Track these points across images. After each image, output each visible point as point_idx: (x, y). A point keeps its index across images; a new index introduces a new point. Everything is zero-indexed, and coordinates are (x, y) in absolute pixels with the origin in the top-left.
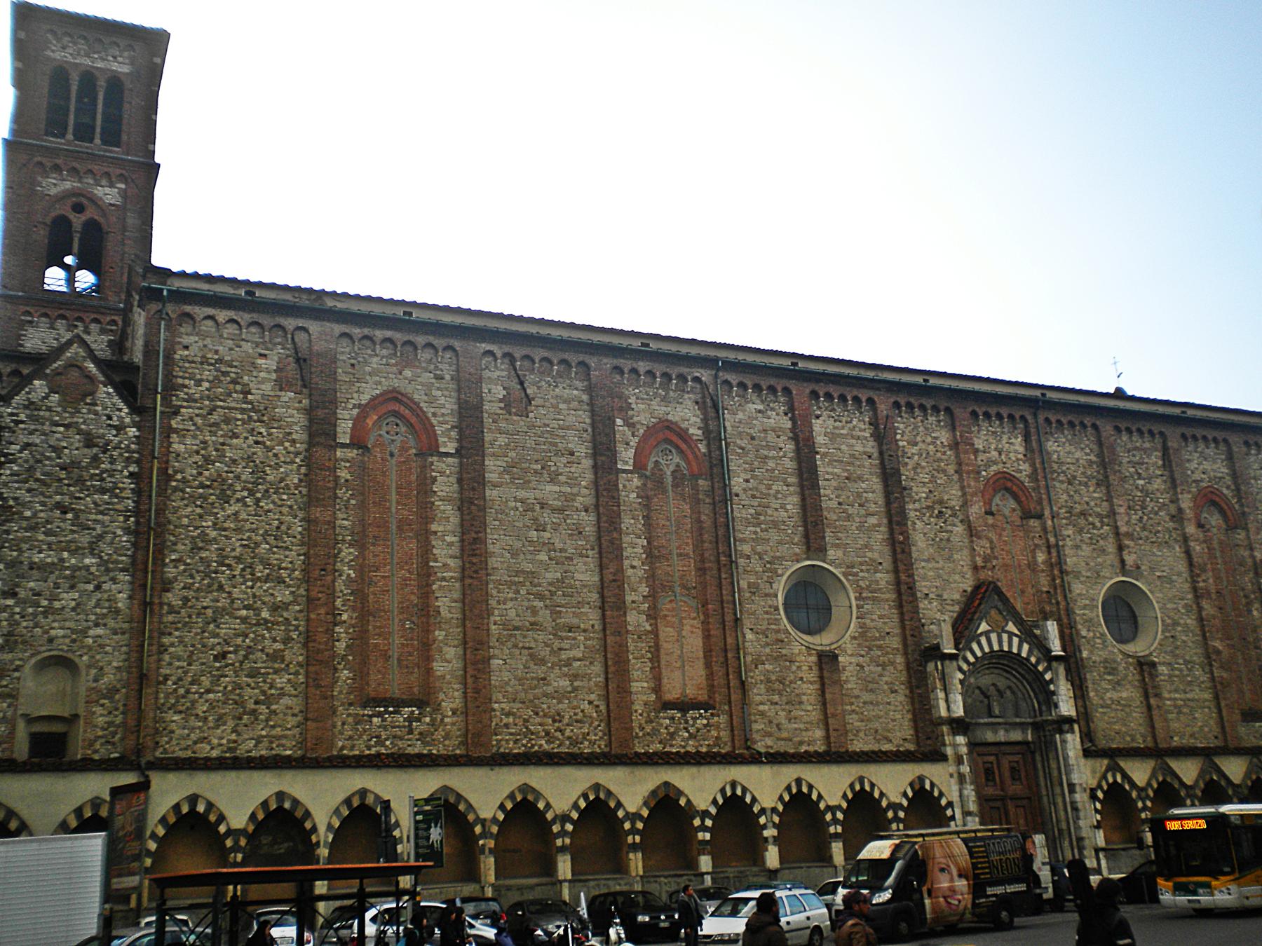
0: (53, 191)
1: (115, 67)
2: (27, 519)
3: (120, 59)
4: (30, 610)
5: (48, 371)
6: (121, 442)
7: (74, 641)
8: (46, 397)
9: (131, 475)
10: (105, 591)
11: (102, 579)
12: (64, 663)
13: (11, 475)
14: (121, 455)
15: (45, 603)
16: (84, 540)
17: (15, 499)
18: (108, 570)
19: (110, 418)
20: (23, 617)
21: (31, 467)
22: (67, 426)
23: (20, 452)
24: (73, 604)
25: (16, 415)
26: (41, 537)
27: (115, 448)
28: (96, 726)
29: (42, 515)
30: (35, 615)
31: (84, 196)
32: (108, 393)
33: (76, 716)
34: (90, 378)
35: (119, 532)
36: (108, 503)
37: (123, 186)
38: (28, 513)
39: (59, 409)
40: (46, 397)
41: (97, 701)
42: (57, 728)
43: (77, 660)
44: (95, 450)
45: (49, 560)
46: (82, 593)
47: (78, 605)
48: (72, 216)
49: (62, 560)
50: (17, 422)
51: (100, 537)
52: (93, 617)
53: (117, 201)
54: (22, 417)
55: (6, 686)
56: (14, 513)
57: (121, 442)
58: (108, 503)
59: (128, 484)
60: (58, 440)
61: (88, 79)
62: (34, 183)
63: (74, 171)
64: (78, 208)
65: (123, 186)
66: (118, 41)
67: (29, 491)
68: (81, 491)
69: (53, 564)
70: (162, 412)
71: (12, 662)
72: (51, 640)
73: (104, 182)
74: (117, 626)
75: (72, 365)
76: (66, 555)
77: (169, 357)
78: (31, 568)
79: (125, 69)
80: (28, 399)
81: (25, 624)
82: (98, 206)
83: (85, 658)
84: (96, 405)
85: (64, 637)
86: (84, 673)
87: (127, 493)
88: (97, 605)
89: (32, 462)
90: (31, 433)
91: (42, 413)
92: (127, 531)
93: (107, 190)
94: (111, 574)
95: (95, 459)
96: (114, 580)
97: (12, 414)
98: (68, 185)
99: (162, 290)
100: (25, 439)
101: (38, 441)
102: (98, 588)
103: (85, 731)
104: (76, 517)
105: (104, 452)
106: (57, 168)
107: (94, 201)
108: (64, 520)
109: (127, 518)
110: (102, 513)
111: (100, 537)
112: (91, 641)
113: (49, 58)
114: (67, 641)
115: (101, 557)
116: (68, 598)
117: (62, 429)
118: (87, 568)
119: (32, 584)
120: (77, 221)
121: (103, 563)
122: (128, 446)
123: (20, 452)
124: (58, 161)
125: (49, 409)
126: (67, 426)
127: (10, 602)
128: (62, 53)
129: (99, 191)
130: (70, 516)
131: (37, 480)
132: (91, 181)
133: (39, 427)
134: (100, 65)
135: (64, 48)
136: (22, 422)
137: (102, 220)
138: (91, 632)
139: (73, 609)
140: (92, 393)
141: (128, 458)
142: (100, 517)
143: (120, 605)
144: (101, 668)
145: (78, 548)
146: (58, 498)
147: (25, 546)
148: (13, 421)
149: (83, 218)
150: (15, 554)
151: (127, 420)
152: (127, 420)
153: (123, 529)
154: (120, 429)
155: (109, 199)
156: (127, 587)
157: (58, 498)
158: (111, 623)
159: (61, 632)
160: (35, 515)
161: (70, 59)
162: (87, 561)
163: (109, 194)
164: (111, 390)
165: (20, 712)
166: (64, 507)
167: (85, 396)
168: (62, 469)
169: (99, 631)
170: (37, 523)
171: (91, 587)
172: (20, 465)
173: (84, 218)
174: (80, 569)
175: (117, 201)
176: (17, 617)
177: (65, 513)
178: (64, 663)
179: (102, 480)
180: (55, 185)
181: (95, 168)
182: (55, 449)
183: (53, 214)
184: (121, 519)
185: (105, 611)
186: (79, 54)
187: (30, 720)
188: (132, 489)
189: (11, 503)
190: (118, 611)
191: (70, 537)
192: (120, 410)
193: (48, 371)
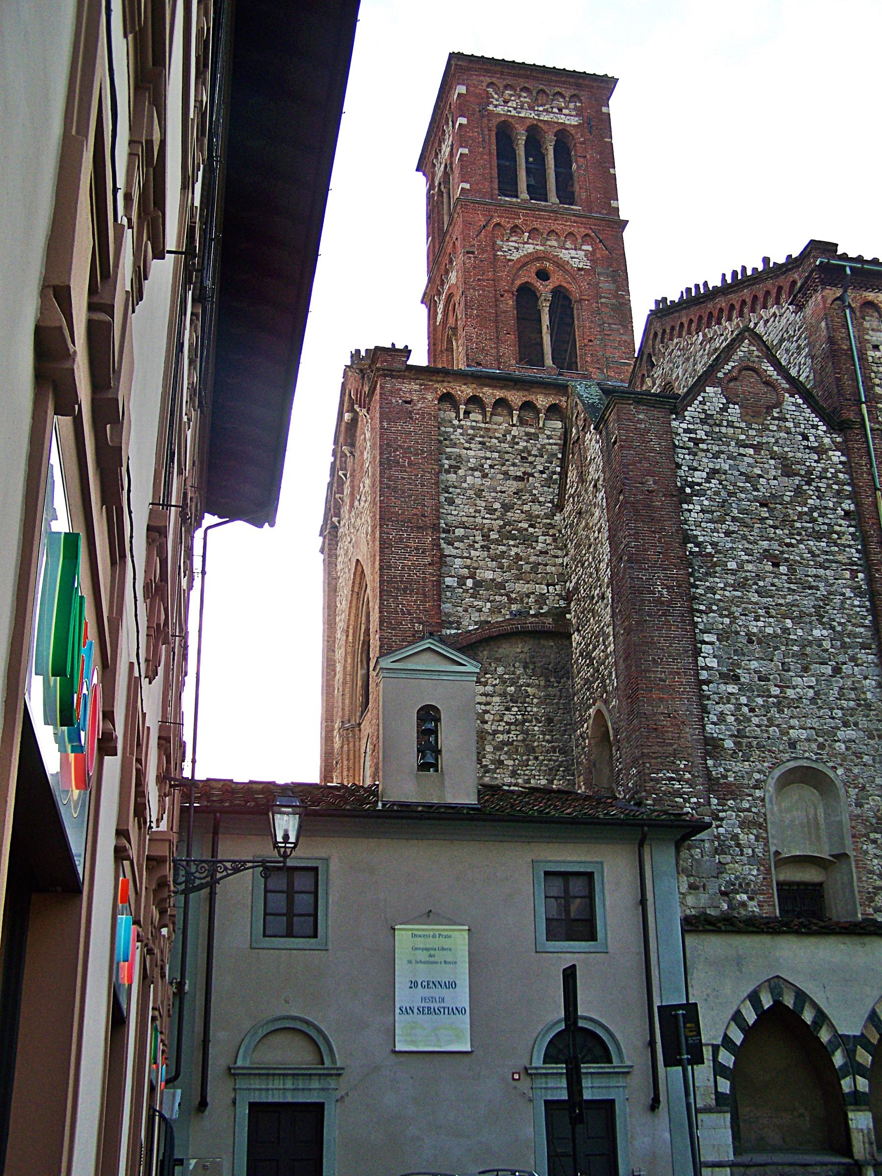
0: (516, 256)
1: (562, 119)
2: (733, 572)
3: (565, 111)
4: (760, 701)
5: (720, 375)
6: (825, 470)
7: (821, 746)
8: (724, 409)
9: (847, 513)
10: (848, 676)
11: (841, 658)
12: (808, 777)
13: (702, 511)
14: (829, 486)
15: (775, 691)
16: (808, 603)
17: (714, 544)
18: (844, 645)
19: (806, 438)
20: (752, 710)
21: (724, 501)
22: (757, 448)
23: (708, 480)
24: (811, 693)
25: (693, 431)
26: (755, 598)
27: (820, 478)
28: (872, 872)
29: (750, 567)
30: (766, 707)
31: (548, 260)
32: (798, 406)
33: (842, 857)
34: (769, 383)
35: (848, 593)
36: (827, 553)
37: (589, 248)
38: (732, 565)
39: (743, 425)
40: (724, 409)
41: (866, 835)
42: (810, 875)
43: (832, 775)
44: (797, 480)
45: (769, 630)
46: (819, 676)
47: (817, 693)
48: (538, 284)
49: (785, 630)
50: (697, 442)
51: (826, 599)
52: (840, 713)
53: (585, 264)
54: (701, 434)
55: (749, 810)
56: (715, 565)
57: (825, 470)
58: (827, 553)
59: (846, 528)
60: (749, 465)
61: (534, 133)
62: (494, 248)
63: (534, 232)
64: (543, 275)
65: (589, 248)
66: (563, 91)
67: (728, 534)
68: (791, 535)
69: (776, 636)
70: (872, 430)
71: (750, 774)
72: (793, 745)
73: (568, 245)
74: (872, 727)
75: (747, 368)
76: (789, 623)
77: (863, 358)
78: (750, 641)
79: (574, 121)
80: (704, 411)
81: (755, 720)
82: (566, 271)
83: (840, 771)
84: (786, 420)
85: (808, 740)
86: (842, 792)
87: (847, 540)
88: (841, 696)
89: (724, 494)
90: (716, 456)
91: (724, 430)
92: (857, 591)
93: (573, 252)
94: (850, 652)
95: (798, 491)
96: (853, 659)
97: (686, 431)
98: (530, 248)
99: (845, 267)
100: (707, 463)
101: (727, 467)
102: (837, 670)
103: (860, 879)
104: (792, 571)
105: (808, 483)
106: (515, 230)
107: (561, 265)
108: (777, 575)
109: (854, 577)
110: (821, 566)
111: (826, 599)
112: (843, 746)
113: (491, 113)
114: (814, 746)
115: (833, 628)
116: (802, 685)
117: (751, 451)
118: (819, 642)
119: (754, 665)
120: (544, 289)
121: (837, 636)
122: (835, 475)
123: (708, 480)
124: (519, 222)
125: (730, 424)
126: (757, 448)
127: (732, 688)
128: (508, 106)
129: (564, 255)
130: (783, 569)
131: (734, 519)
132: (555, 243)
133: (723, 448)
134: (545, 117)
135: (506, 102)
136: (703, 441)
137: (573, 288)
138: (840, 734)
139: (813, 701)
140: (779, 404)
141: (838, 492)
142: (821, 572)
143: (869, 695)
144: (864, 787)
145: (802, 614)
146: (765, 544)
147: (737, 611)
148: (690, 439)
149: (551, 285)
150: (727, 621)
151: (827, 441)
152: (827, 441)
153: (853, 589)
154: (821, 451)
155: (575, 263)
156: (872, 671)
157: (765, 544)
158: (863, 723)
159: (804, 734)
160: (741, 566)
161: (513, 113)
162: (817, 633)
163: (575, 257)
164: (800, 401)
165: (773, 849)
166: (776, 557)
167: (769, 409)
168: (762, 505)
169: (850, 733)
170: (746, 579)
171: (828, 670)
172: (710, 499)
173: (551, 287)
174: (810, 644)
175: (585, 264)
176: (745, 709)
177: (776, 565)
178: (808, 777)
179: (813, 520)
180: (517, 249)
181: (557, 227)
182: (748, 478)
183: (518, 282)
184: (847, 574)
185: (852, 704)
186: (522, 108)
187: (783, 862)
188: (850, 534)
189: (709, 549)
190: (868, 706)
191: (790, 598)
192: (815, 427)
193: (720, 375)
